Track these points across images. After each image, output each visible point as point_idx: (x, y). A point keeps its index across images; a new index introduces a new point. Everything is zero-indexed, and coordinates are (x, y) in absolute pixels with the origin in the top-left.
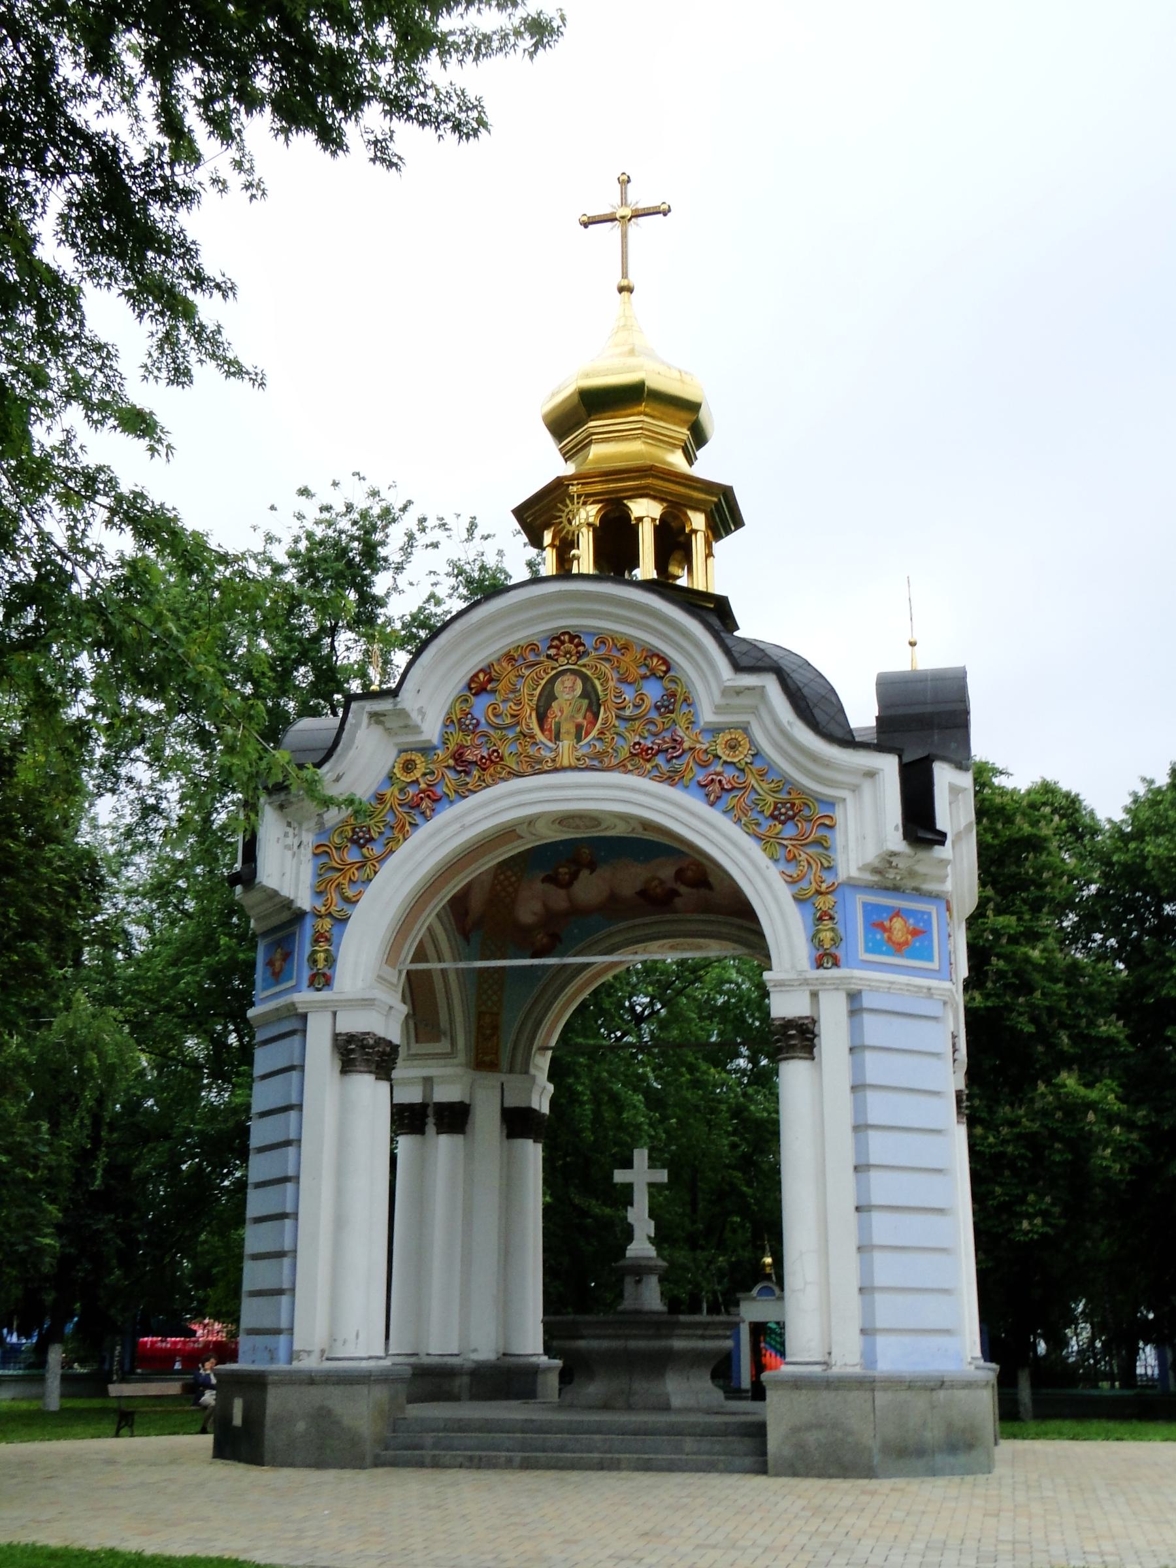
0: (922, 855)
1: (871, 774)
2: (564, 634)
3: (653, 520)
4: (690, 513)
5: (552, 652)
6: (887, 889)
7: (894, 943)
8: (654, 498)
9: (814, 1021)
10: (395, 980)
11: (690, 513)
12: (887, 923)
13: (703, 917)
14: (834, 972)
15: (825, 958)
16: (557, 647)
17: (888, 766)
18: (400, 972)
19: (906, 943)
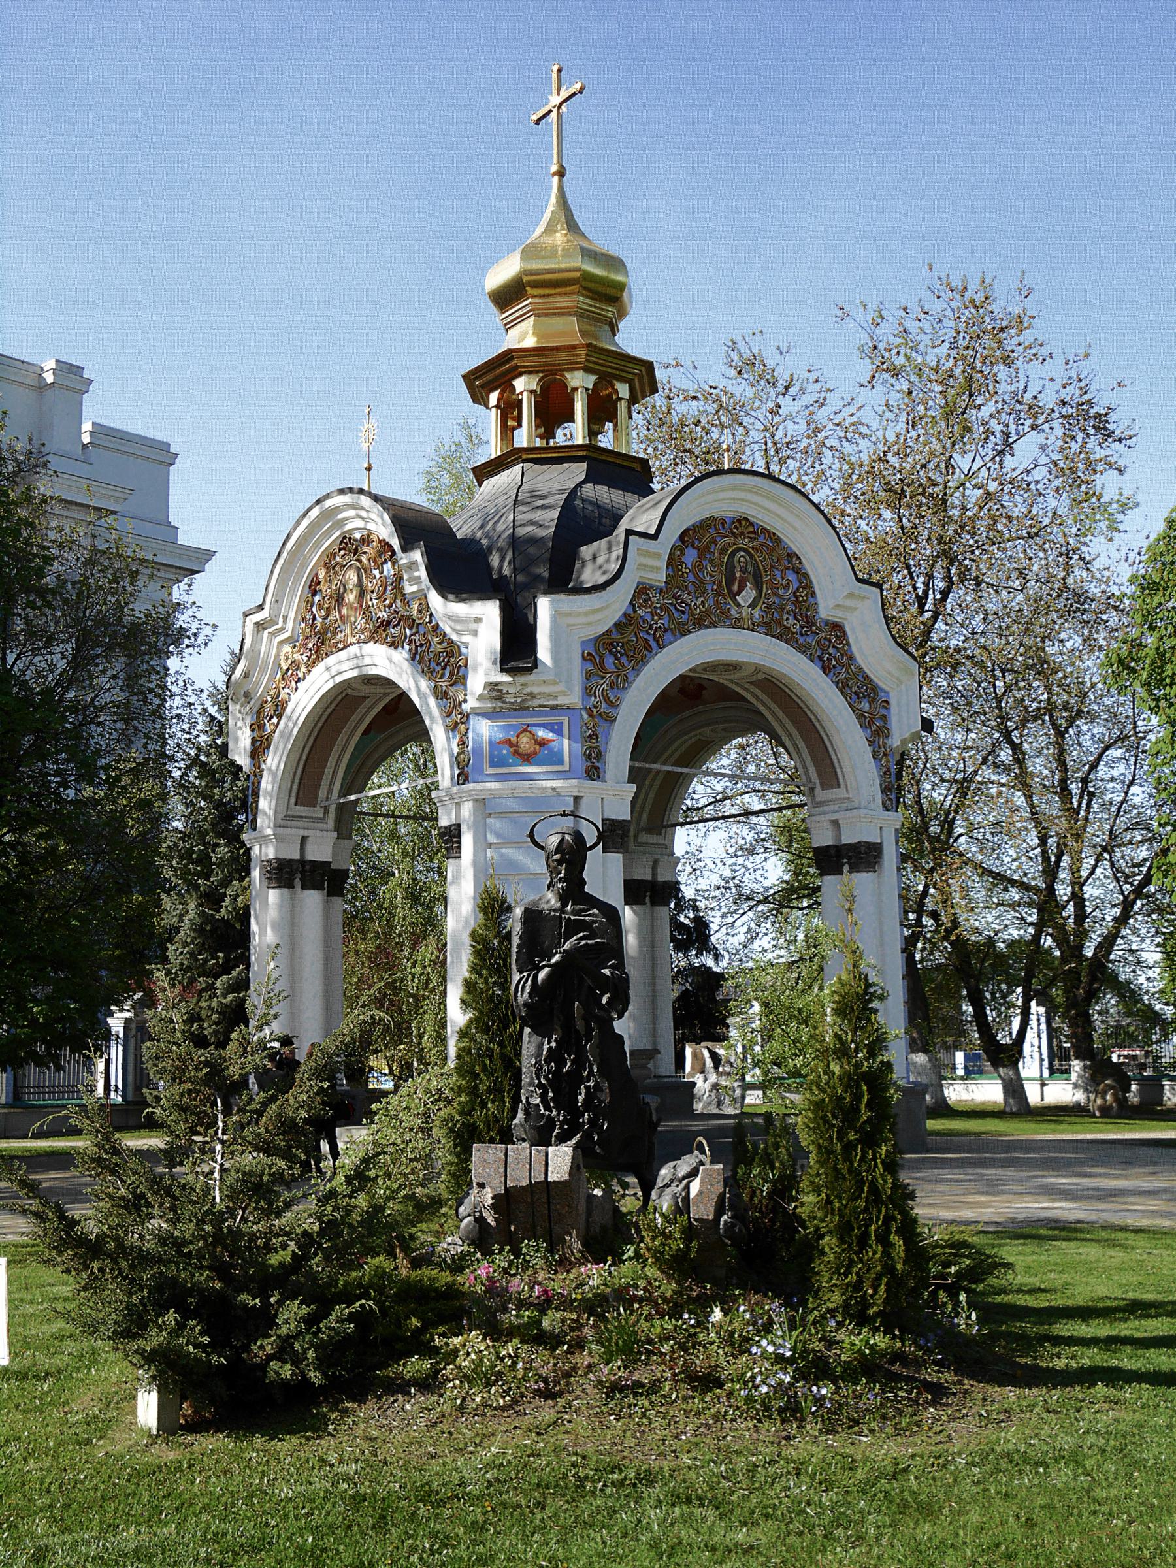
0: (521, 679)
1: (478, 620)
2: (345, 537)
3: (531, 392)
4: (567, 375)
5: (342, 552)
6: (515, 710)
7: (520, 755)
8: (530, 373)
9: (459, 825)
10: (321, 815)
11: (567, 375)
12: (514, 739)
13: (722, 705)
14: (469, 786)
15: (463, 778)
16: (344, 549)
17: (489, 613)
18: (326, 808)
19: (535, 753)
